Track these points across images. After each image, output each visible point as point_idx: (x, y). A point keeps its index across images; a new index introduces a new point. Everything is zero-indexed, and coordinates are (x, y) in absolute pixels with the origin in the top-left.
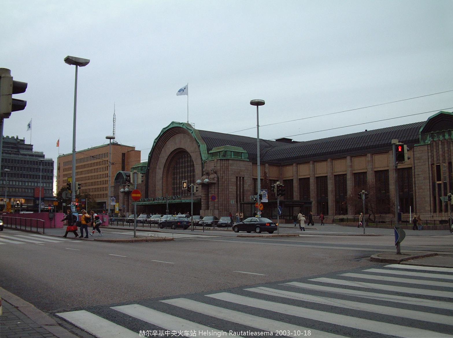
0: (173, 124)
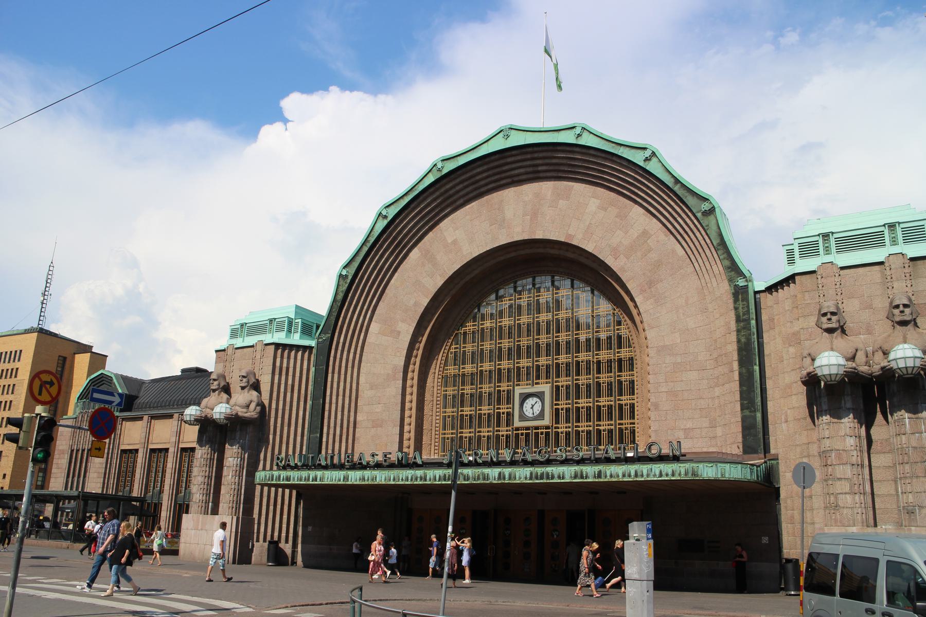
0: (508, 136)
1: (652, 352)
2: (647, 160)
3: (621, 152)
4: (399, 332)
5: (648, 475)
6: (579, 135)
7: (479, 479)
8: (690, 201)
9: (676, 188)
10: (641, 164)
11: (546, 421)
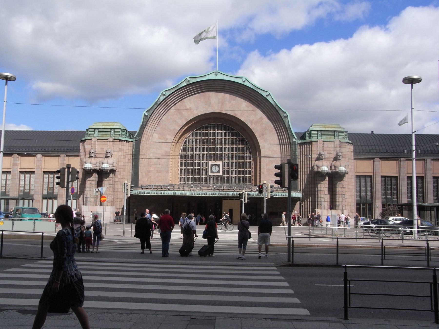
2: (267, 95)
3: (258, 90)
4: (167, 139)
6: (244, 81)
8: (281, 112)
9: (276, 107)
10: (265, 96)
11: (221, 174)
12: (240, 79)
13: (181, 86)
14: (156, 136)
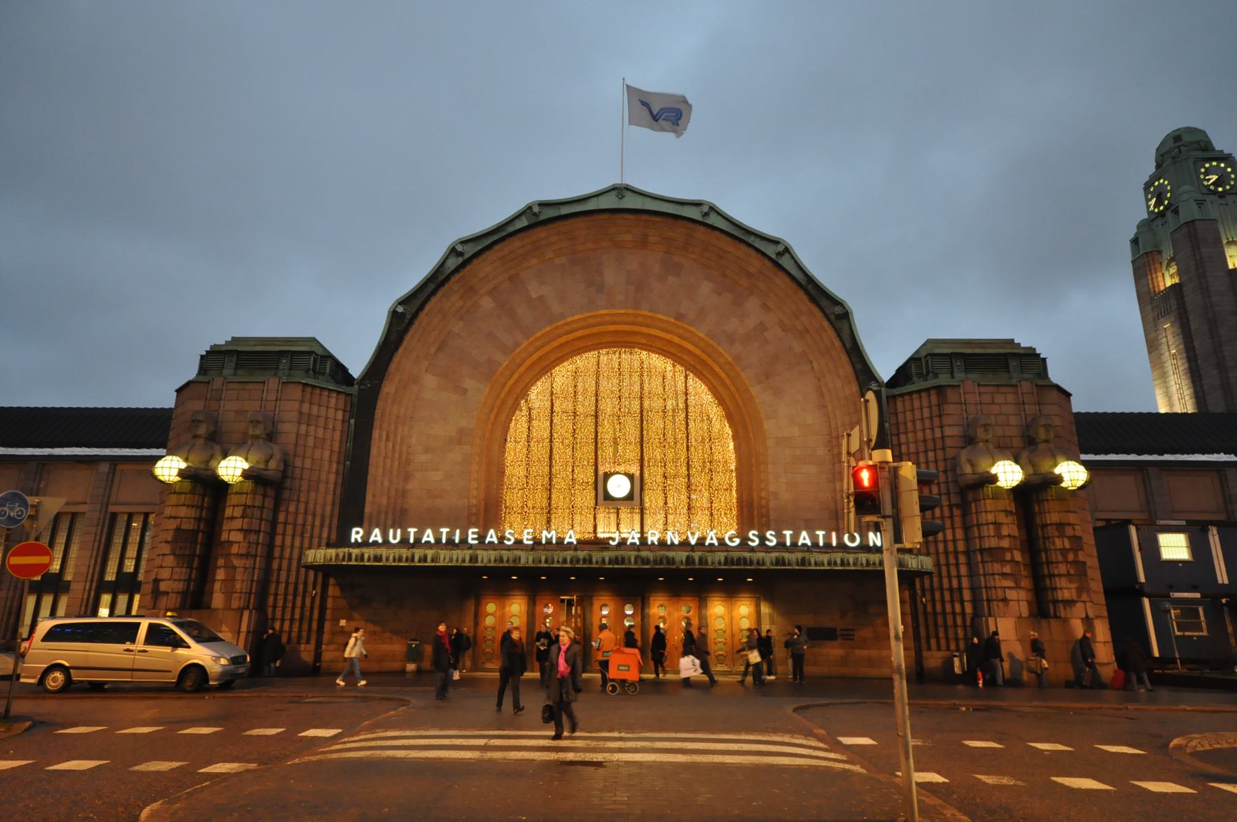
1: (770, 443)
2: (779, 254)
3: (751, 239)
4: (465, 391)
5: (855, 564)
6: (706, 214)
7: (661, 563)
9: (810, 287)
10: (774, 257)
12: (694, 209)
13: (511, 229)
14: (430, 381)
